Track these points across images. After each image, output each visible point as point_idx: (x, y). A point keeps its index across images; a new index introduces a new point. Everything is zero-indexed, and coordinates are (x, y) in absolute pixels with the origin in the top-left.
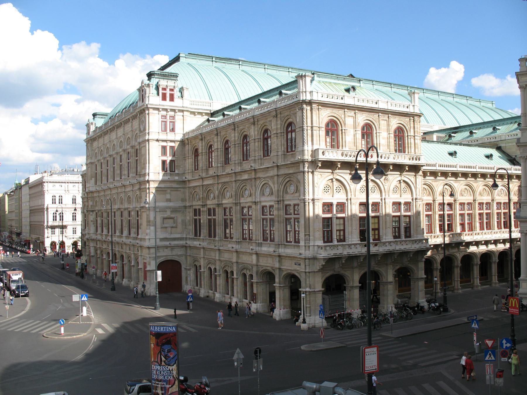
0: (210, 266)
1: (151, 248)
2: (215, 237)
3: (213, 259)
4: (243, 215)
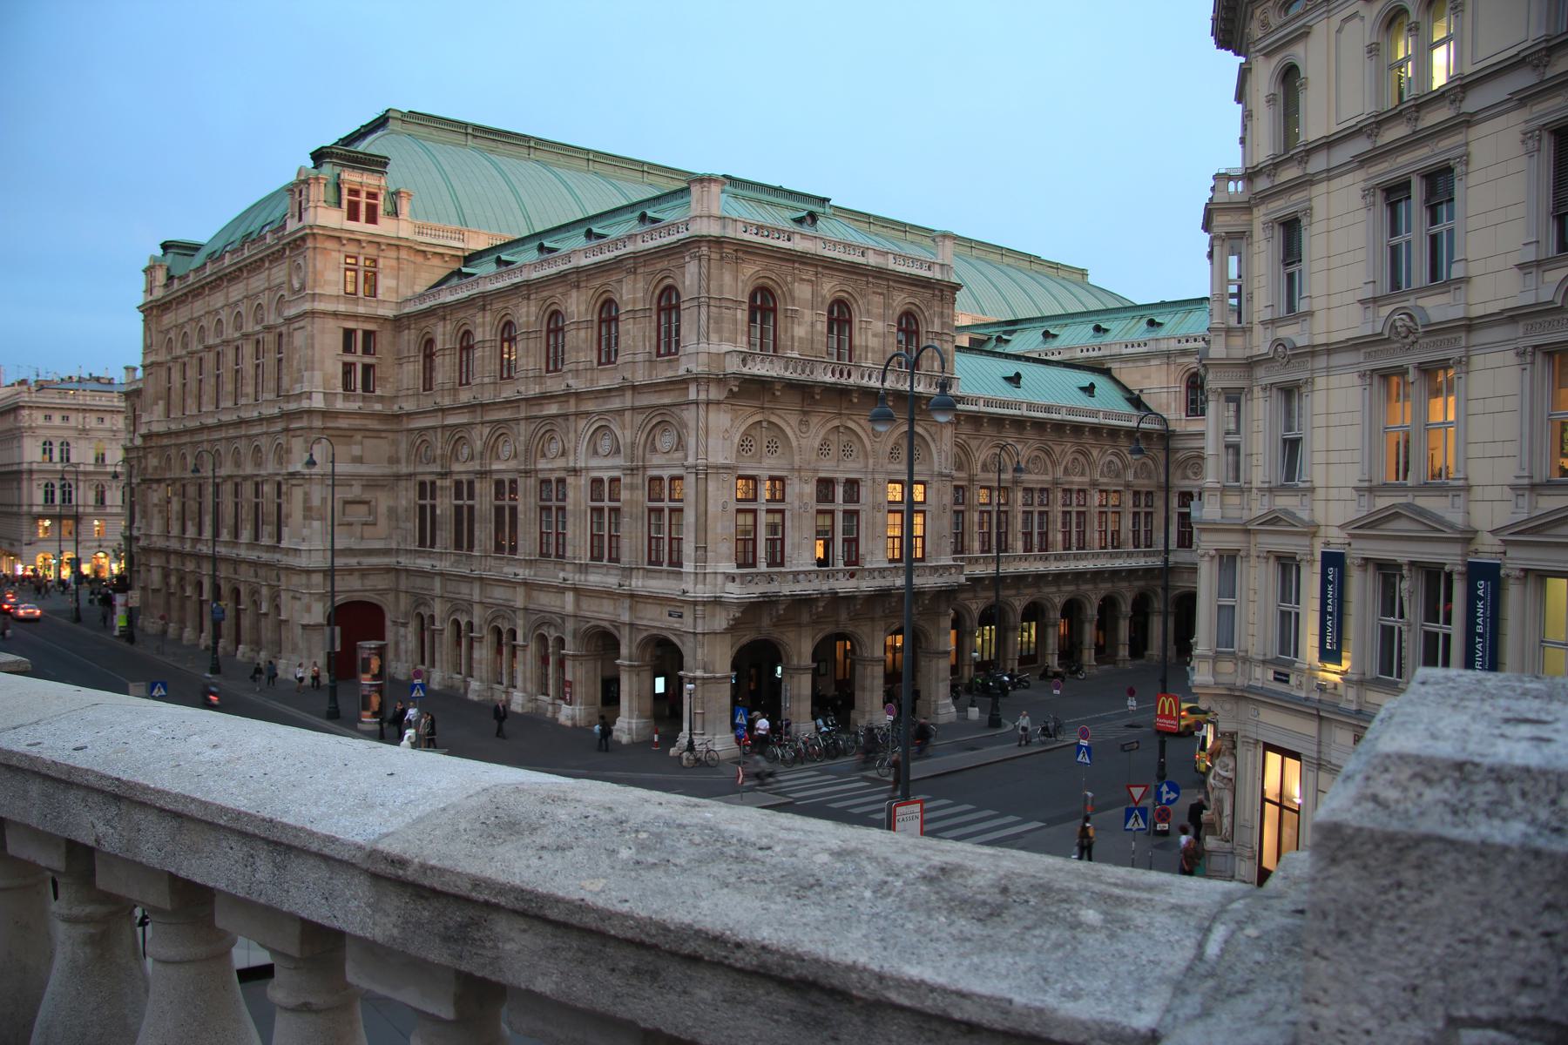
0: (458, 616)
2: (471, 547)
4: (541, 500)
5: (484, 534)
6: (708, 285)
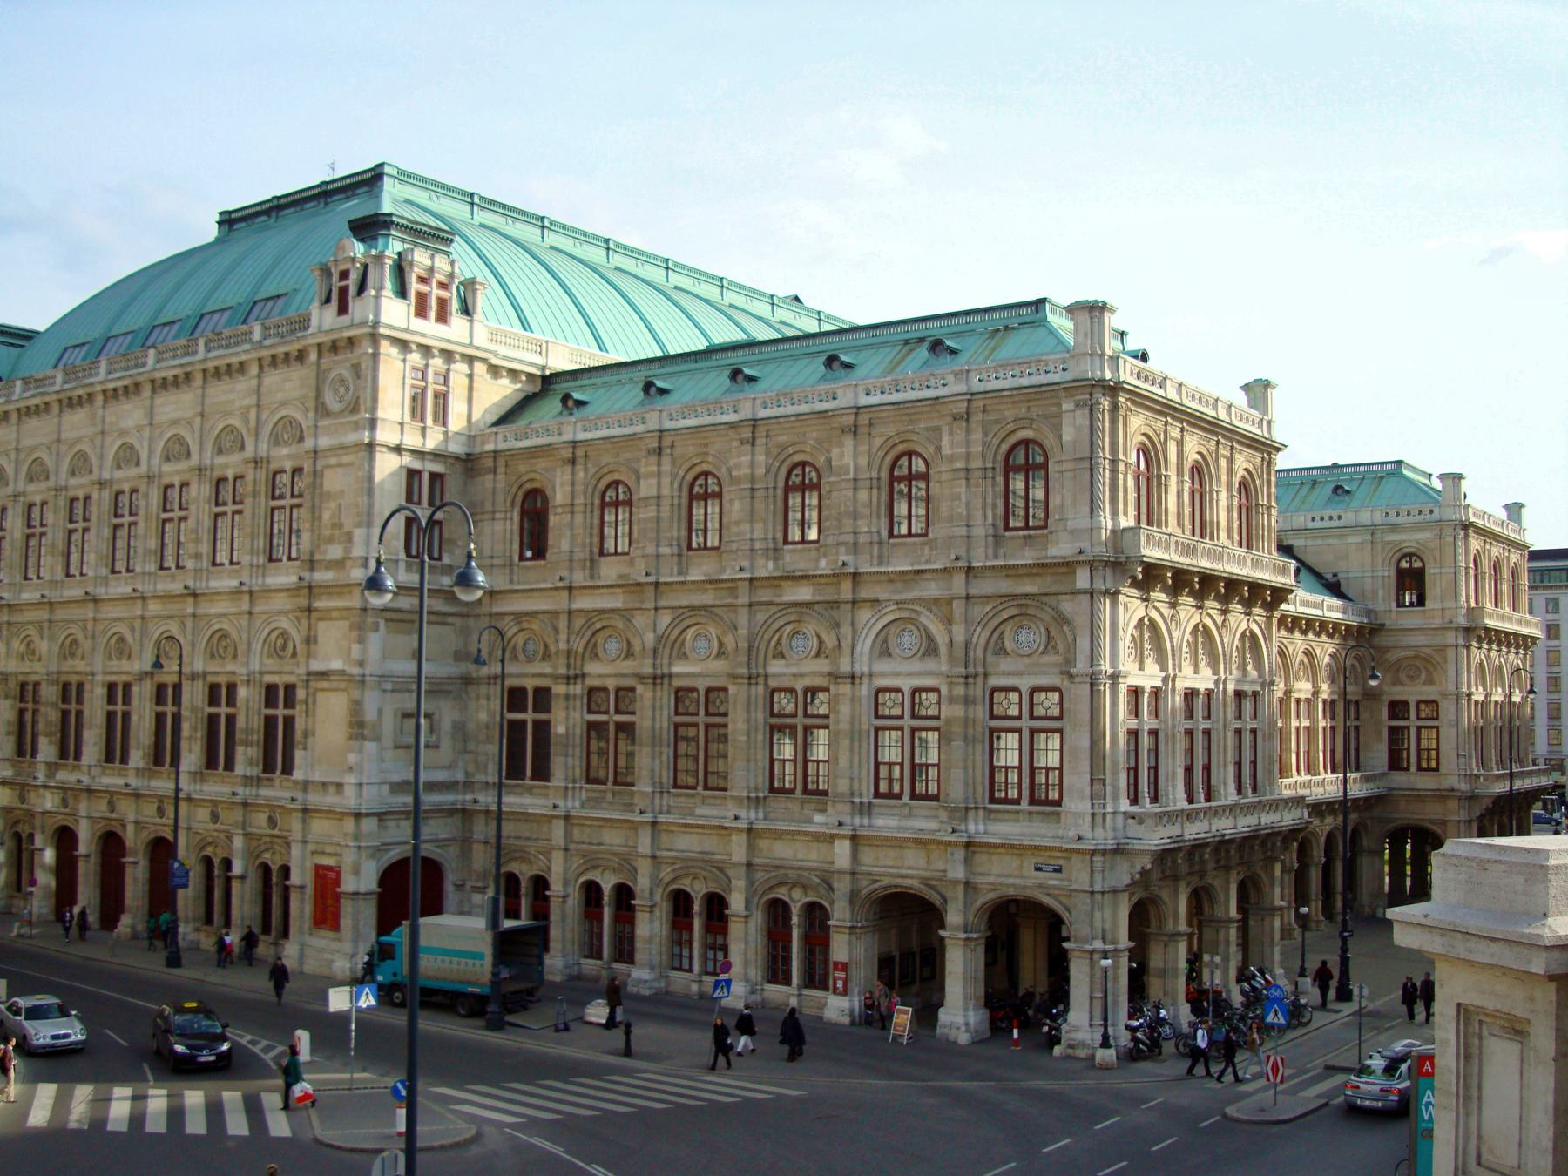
0: (594, 876)
1: (367, 815)
3: (615, 854)
4: (772, 715)
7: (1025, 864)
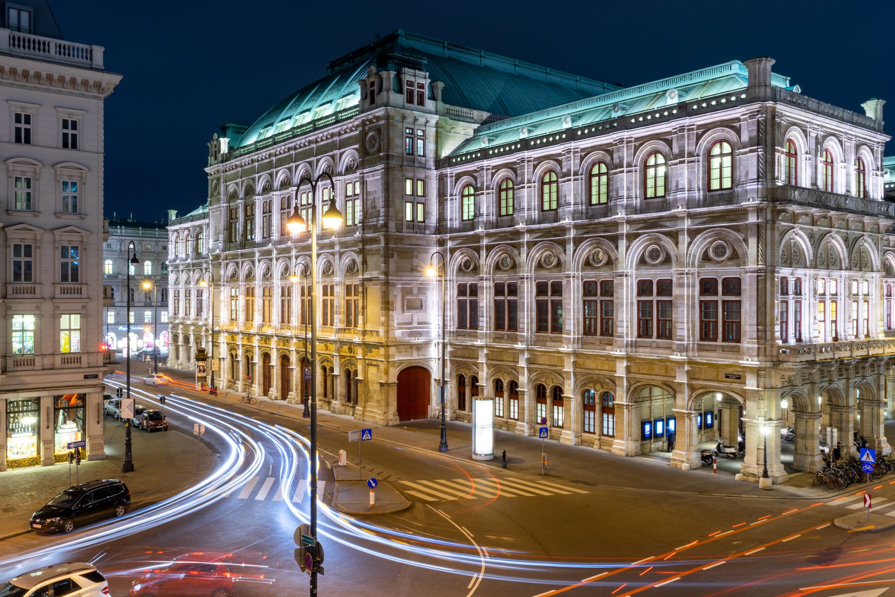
5: (527, 318)
6: (766, 137)
7: (720, 374)
